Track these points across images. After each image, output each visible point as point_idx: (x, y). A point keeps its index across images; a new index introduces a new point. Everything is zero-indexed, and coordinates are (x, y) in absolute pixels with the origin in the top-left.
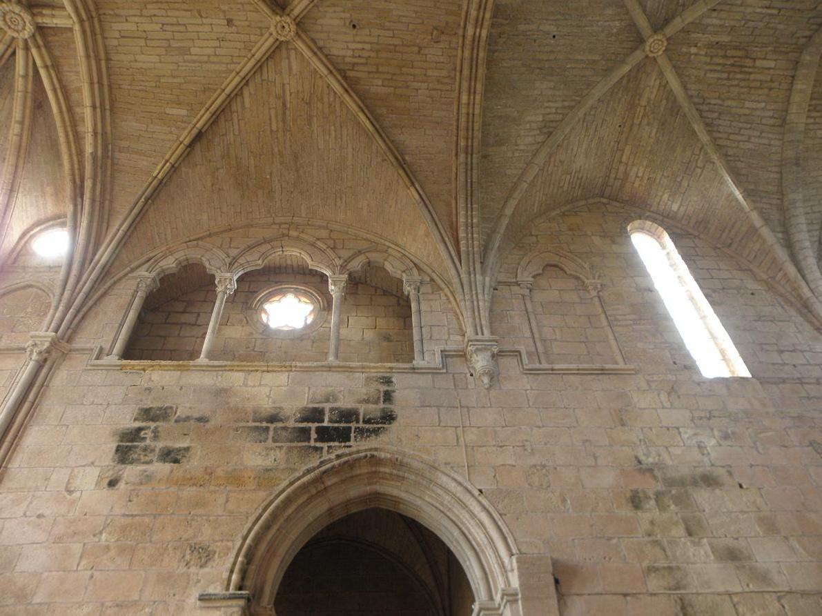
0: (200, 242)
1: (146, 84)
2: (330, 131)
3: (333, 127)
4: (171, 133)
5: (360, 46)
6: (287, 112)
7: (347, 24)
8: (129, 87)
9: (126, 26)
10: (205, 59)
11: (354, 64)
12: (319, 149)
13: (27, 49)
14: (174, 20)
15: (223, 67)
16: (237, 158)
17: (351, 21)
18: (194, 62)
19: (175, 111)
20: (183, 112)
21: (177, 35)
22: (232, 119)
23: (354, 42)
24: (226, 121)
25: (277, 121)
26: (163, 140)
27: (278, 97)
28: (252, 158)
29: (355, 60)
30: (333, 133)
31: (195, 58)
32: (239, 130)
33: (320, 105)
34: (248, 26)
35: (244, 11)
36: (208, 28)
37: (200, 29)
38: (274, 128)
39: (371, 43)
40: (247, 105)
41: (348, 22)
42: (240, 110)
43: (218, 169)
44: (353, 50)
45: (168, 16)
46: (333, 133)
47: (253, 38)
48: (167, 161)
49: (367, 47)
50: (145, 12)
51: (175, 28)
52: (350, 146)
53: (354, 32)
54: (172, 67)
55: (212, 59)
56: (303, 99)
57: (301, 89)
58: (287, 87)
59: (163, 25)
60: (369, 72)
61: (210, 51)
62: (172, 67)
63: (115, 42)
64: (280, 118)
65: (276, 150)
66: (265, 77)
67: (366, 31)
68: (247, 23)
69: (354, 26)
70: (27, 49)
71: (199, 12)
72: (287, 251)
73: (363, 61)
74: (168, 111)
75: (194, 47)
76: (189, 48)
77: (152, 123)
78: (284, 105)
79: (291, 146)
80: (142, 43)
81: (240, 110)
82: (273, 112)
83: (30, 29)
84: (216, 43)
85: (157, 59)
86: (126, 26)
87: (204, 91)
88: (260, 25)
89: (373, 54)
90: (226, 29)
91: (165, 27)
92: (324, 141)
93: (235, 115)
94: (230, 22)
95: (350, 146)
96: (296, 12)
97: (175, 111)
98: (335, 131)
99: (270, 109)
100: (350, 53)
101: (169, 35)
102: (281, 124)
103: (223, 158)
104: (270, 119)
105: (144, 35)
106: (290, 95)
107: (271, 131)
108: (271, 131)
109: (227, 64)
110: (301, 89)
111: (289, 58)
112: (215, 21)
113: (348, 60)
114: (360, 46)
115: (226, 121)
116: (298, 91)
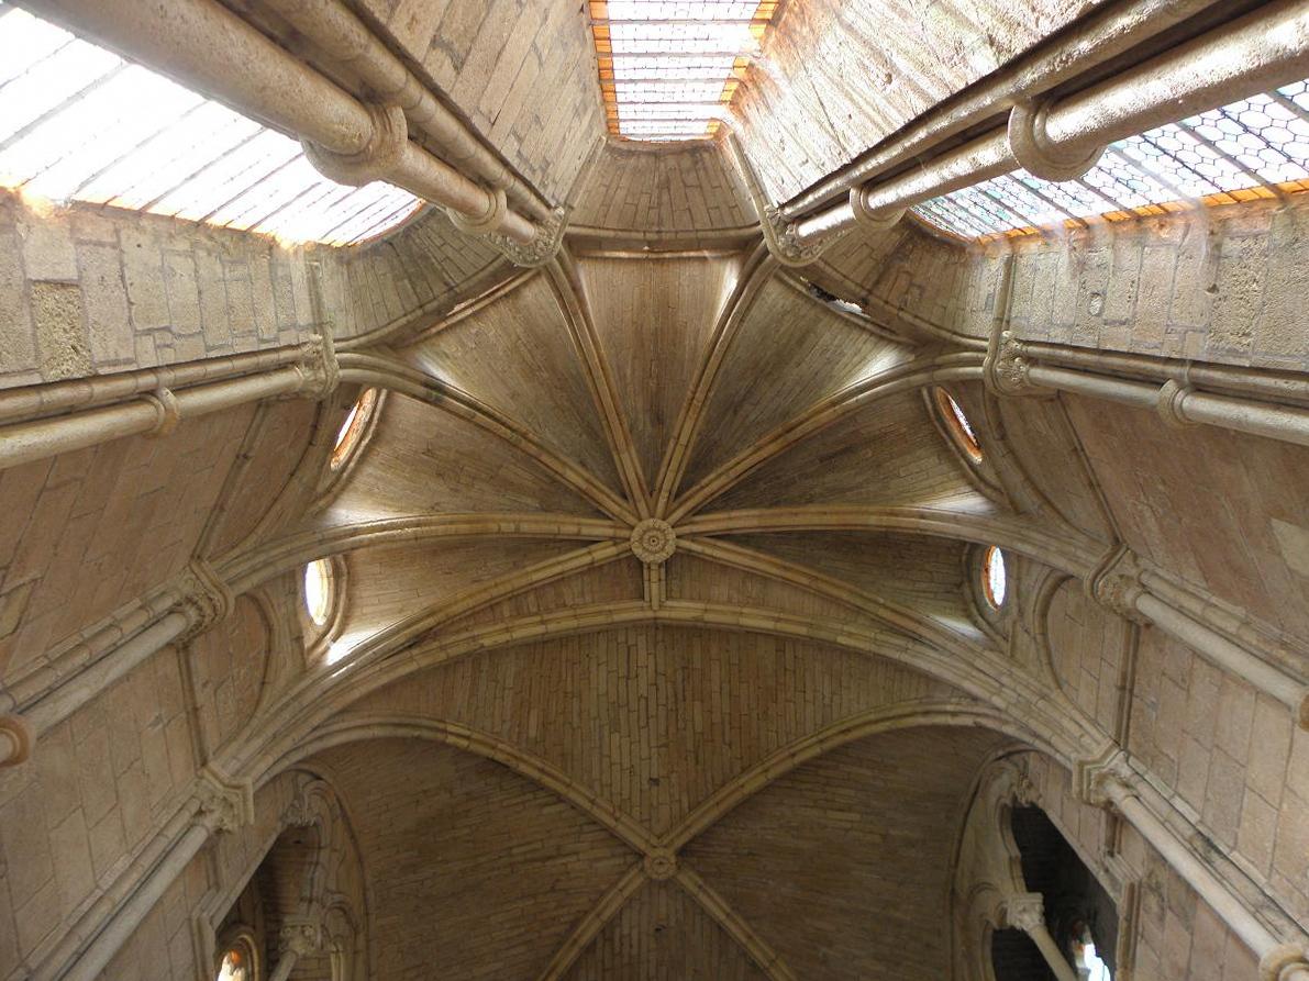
0: (340, 821)
1: (569, 679)
2: (518, 927)
3: (523, 930)
4: (504, 721)
5: (635, 942)
6: (539, 864)
7: (661, 923)
8: (564, 660)
9: (643, 653)
10: (606, 752)
11: (611, 940)
12: (488, 917)
13: (615, 540)
14: (652, 712)
15: (596, 774)
16: (469, 811)
17: (664, 927)
18: (601, 739)
19: (533, 721)
20: (533, 733)
21: (634, 716)
22: (524, 794)
23: (639, 933)
24: (522, 786)
25: (525, 853)
26: (493, 715)
27: (559, 848)
28: (466, 831)
29: (617, 939)
30: (516, 932)
31: (607, 739)
32: (508, 806)
33: (553, 905)
34: (652, 805)
35: (671, 802)
36: (645, 754)
37: (644, 745)
38: (515, 851)
39: (639, 955)
40: (547, 810)
41: (664, 923)
42: (538, 801)
43: (451, 792)
44: (630, 935)
45: (658, 705)
46: (516, 932)
47: (636, 812)
48: (468, 738)
49: (635, 951)
50: (661, 681)
51: (643, 713)
52: (499, 965)
53: (652, 931)
54: (594, 713)
55: (606, 760)
56: (558, 880)
57: (572, 875)
58: (575, 858)
59: (647, 699)
60: (603, 962)
61: (615, 757)
62: (594, 713)
63: (621, 639)
64: (529, 856)
65: (482, 860)
66: (586, 828)
67: (653, 946)
68: (655, 804)
69: (657, 930)
70: (615, 540)
71: (666, 745)
72: (338, 958)
73: (617, 950)
74: (534, 713)
75: (621, 737)
76: (619, 732)
77: (516, 694)
78: (549, 858)
79: (489, 878)
80: (623, 672)
81: (538, 801)
82: (538, 845)
83: (647, 558)
84: (626, 765)
85: (602, 689)
86: (643, 653)
87: (563, 755)
88: (654, 820)
89: (626, 960)
90: (645, 776)
91: (643, 701)
92: (501, 923)
93: (530, 796)
94: (654, 781)
95: (499, 965)
96: (680, 877)
97: (533, 721)
98: (519, 935)
99: (542, 840)
100: (626, 932)
101: (634, 706)
102: (520, 858)
103: (467, 794)
104: (529, 843)
105: (633, 674)
106: (563, 864)
107: (511, 848)
108: (511, 848)
109: (601, 780)
110: (572, 875)
111: (613, 856)
112: (654, 761)
113: (617, 931)
114: (635, 942)
115: (522, 786)
116: (568, 873)
